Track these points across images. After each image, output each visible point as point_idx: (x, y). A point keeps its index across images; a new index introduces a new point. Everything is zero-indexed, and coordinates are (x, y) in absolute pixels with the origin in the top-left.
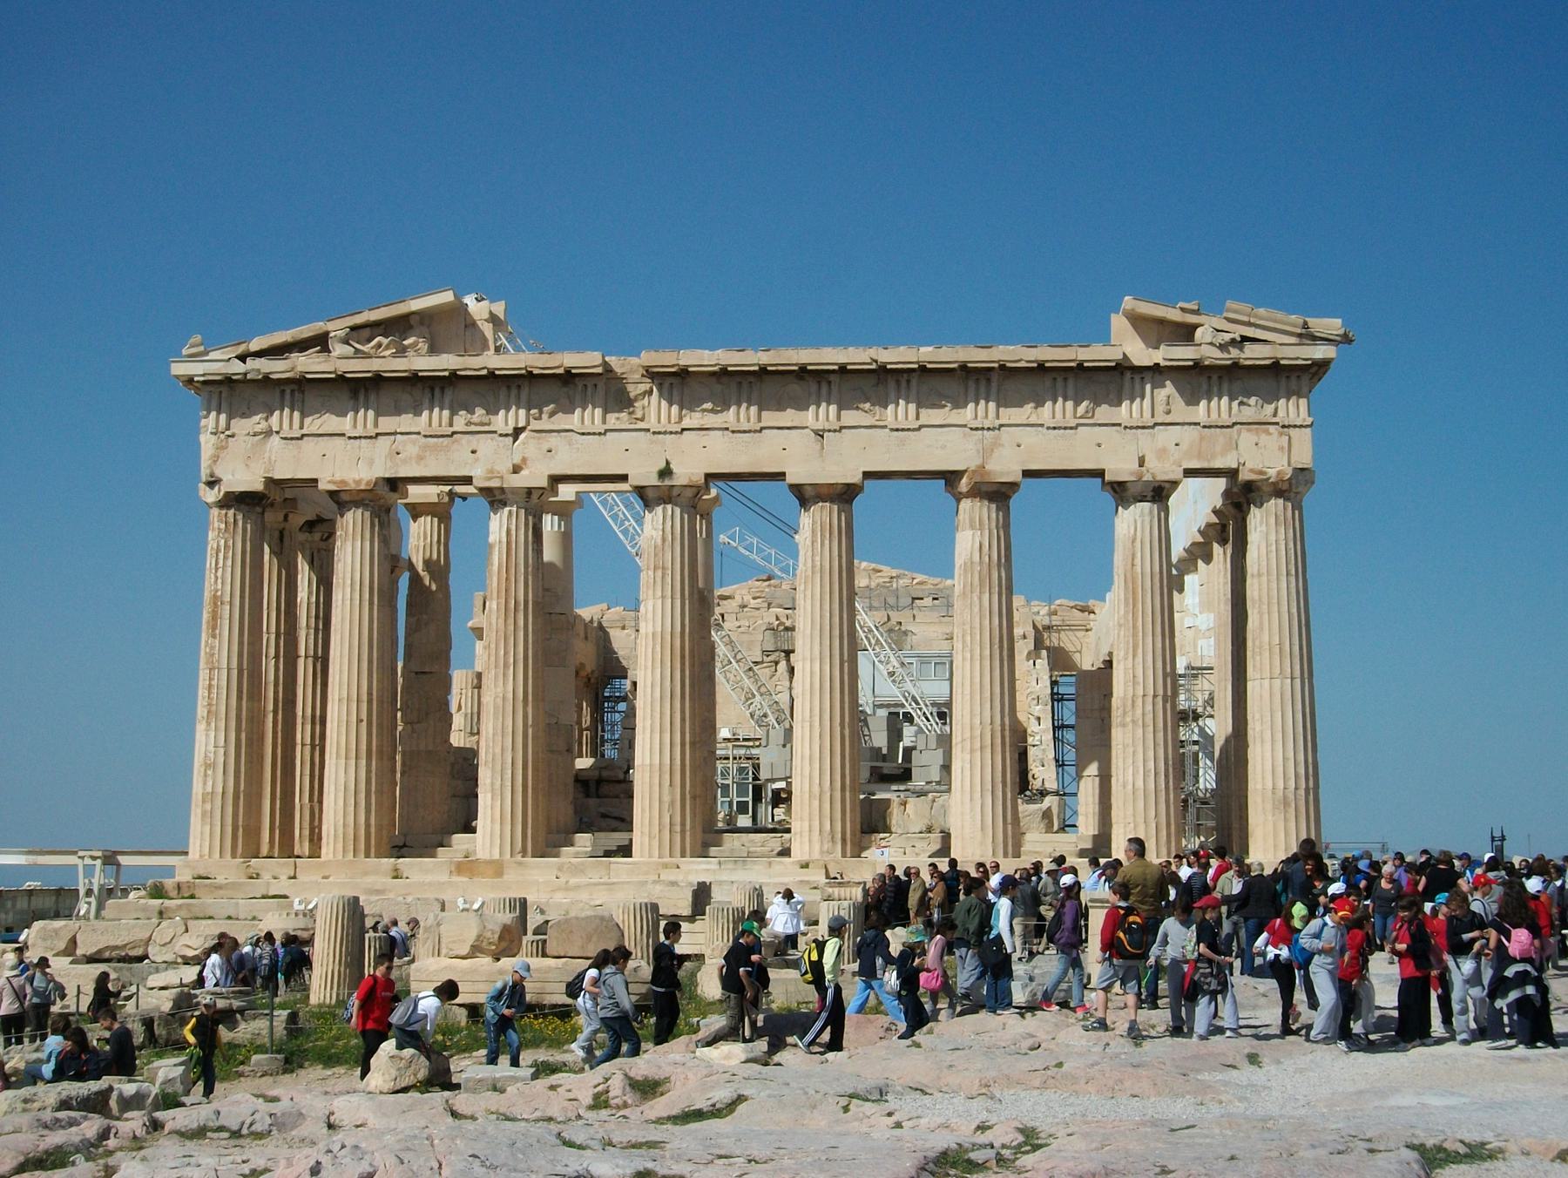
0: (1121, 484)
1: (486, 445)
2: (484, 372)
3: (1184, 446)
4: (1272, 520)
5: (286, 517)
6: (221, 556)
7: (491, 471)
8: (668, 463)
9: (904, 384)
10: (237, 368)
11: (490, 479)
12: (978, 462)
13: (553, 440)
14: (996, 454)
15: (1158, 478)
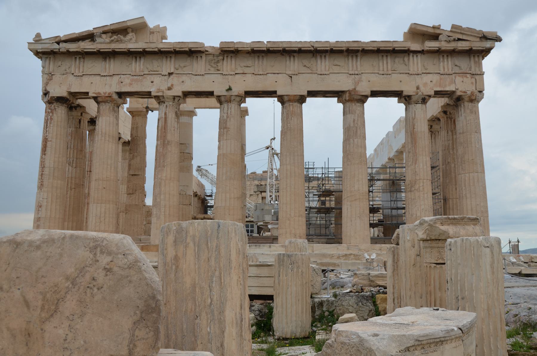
0: (409, 97)
1: (157, 80)
2: (156, 50)
3: (434, 82)
4: (468, 111)
5: (82, 114)
6: (49, 123)
7: (159, 89)
8: (230, 86)
9: (323, 57)
10: (56, 46)
11: (158, 92)
12: (353, 87)
13: (184, 78)
14: (360, 85)
15: (424, 94)
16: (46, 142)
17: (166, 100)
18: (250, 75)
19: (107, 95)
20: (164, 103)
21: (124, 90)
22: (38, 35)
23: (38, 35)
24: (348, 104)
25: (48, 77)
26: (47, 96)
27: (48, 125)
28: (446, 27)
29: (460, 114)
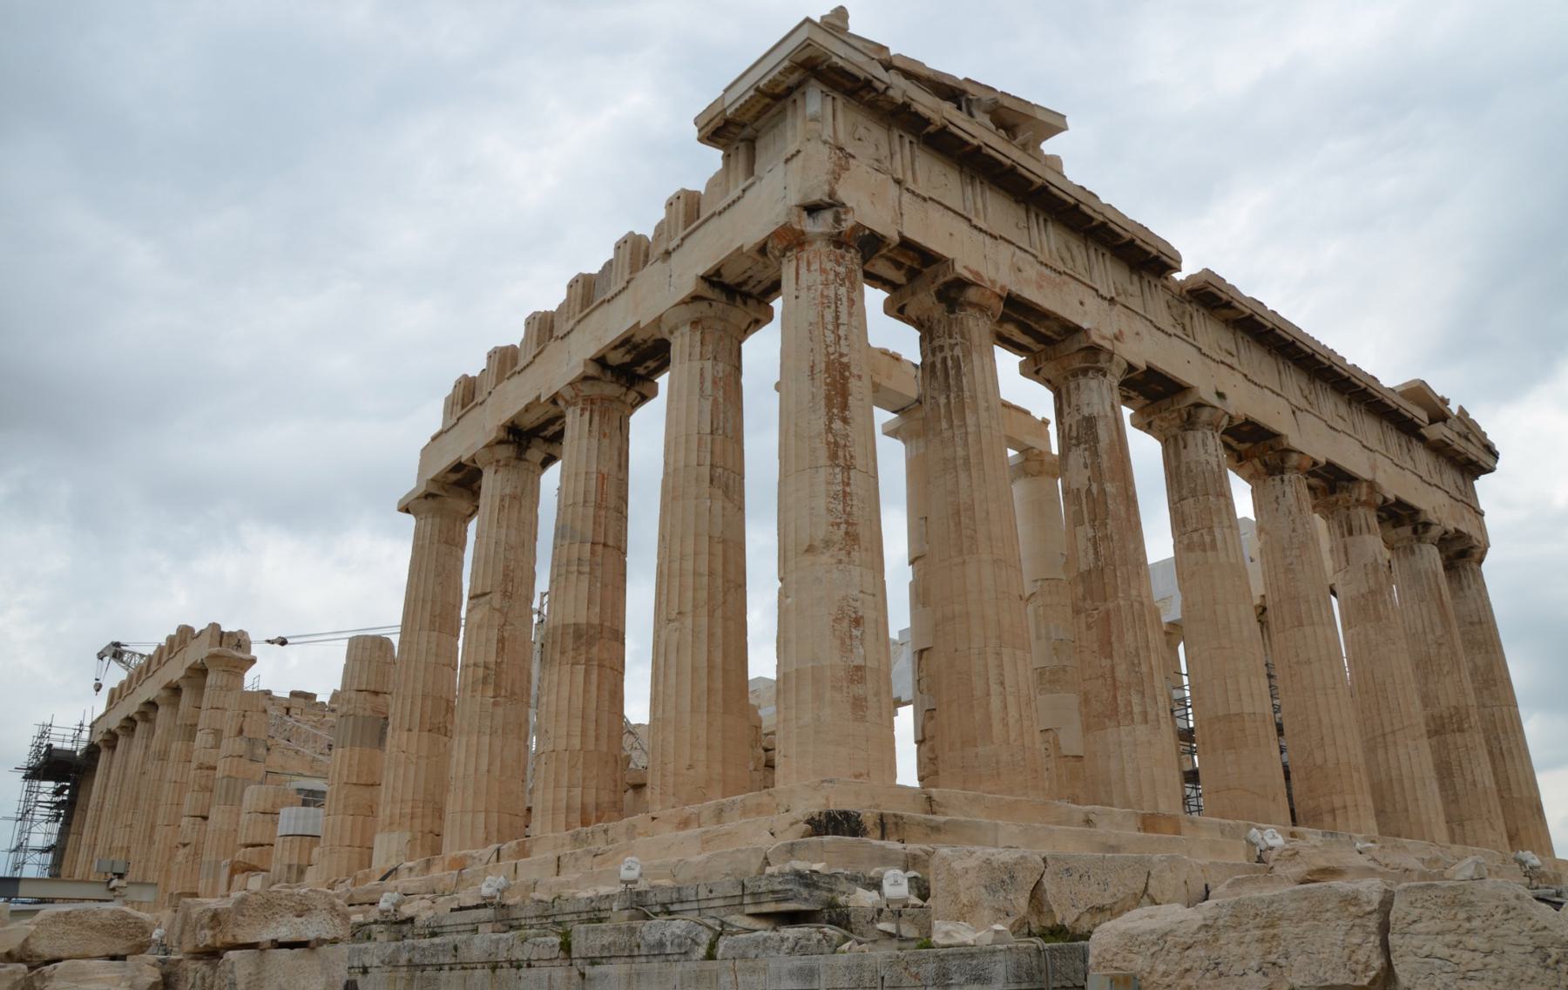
0: (1427, 525)
1: (1092, 301)
2: (1101, 218)
6: (843, 309)
10: (879, 72)
13: (1139, 325)
16: (846, 379)
17: (1114, 368)
18: (1240, 377)
19: (997, 290)
20: (1105, 375)
21: (1030, 294)
22: (841, 13)
23: (841, 13)
24: (1361, 511)
25: (835, 158)
26: (828, 216)
27: (844, 318)
28: (1454, 408)
29: (1465, 582)
